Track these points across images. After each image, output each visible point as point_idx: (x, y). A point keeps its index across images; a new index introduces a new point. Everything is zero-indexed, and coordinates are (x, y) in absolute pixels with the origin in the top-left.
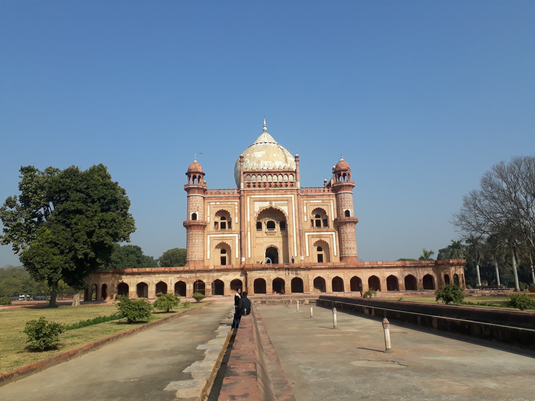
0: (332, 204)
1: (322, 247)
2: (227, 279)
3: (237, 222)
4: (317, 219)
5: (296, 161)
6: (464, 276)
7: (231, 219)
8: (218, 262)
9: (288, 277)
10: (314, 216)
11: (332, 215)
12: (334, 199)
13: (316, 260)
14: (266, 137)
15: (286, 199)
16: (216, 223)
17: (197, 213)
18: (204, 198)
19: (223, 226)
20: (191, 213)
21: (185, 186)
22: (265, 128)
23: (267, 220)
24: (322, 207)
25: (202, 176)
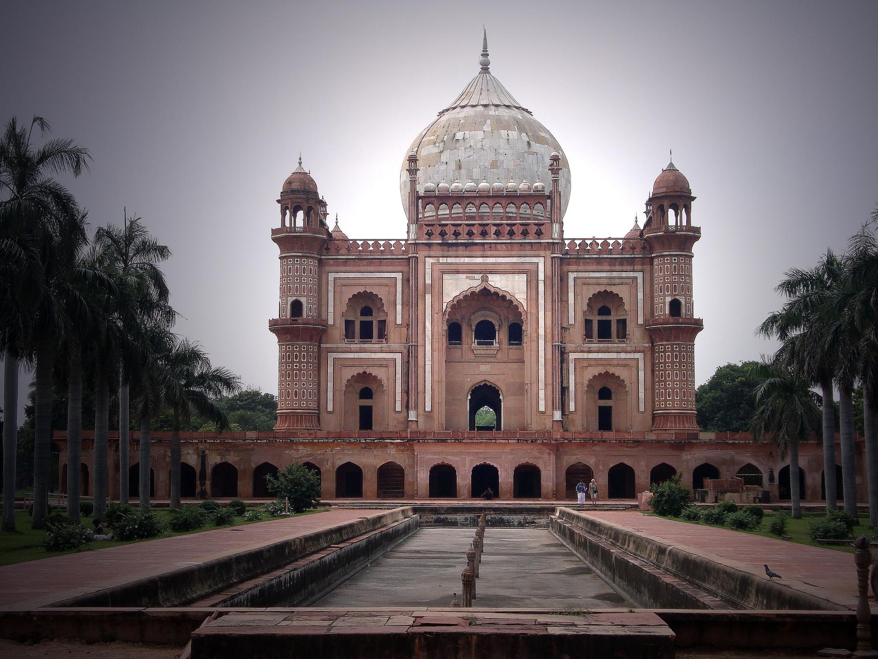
0: (640, 281)
2: (370, 461)
3: (399, 321)
4: (604, 318)
9: (506, 464)
10: (596, 312)
11: (636, 309)
17: (303, 300)
18: (320, 260)
20: (291, 300)
23: (477, 319)
24: (615, 290)
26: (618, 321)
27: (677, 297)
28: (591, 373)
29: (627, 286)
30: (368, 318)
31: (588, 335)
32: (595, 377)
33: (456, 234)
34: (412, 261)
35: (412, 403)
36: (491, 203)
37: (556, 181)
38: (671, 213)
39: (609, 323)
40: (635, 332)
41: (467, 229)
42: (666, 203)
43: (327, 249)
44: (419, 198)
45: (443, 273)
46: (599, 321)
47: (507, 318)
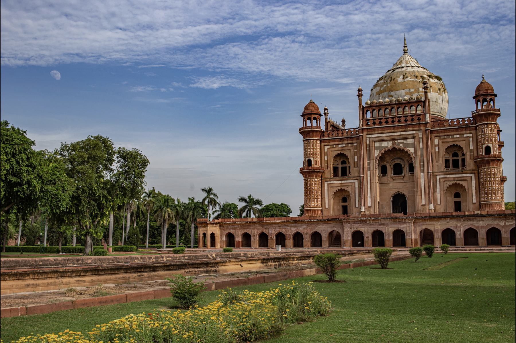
4: (455, 158)
10: (451, 156)
13: (451, 210)
15: (412, 136)
17: (312, 159)
18: (321, 141)
26: (462, 159)
29: (464, 142)
30: (344, 166)
31: (447, 166)
34: (361, 138)
37: (426, 93)
39: (458, 160)
40: (470, 164)
43: (324, 135)
44: (363, 108)
46: (453, 160)
47: (408, 161)
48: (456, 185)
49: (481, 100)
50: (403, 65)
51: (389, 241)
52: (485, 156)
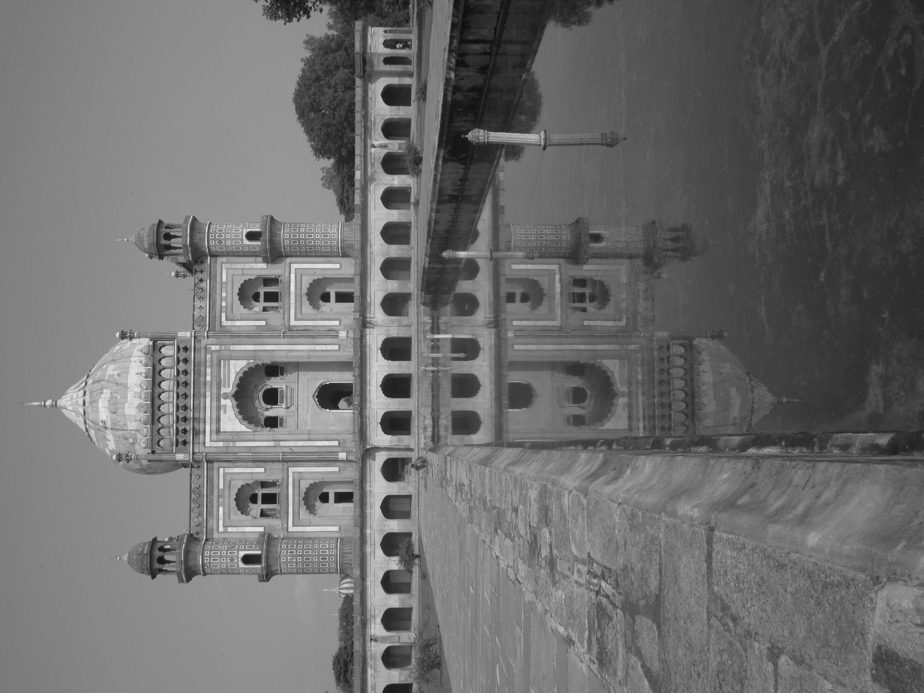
1: (319, 293)
3: (262, 470)
5: (131, 338)
6: (388, 29)
7: (256, 482)
8: (347, 507)
12: (220, 260)
14: (70, 402)
16: (263, 514)
17: (242, 554)
19: (270, 499)
20: (241, 565)
21: (181, 580)
22: (49, 403)
24: (237, 286)
25: (159, 545)
27: (244, 234)
28: (307, 308)
32: (311, 304)
33: (185, 419)
35: (331, 457)
36: (157, 391)
38: (174, 242)
39: (265, 293)
41: (181, 411)
42: (163, 242)
43: (198, 533)
44: (153, 452)
45: (218, 431)
46: (265, 301)
48: (310, 295)
49: (163, 242)
50: (81, 402)
51: (400, 366)
52: (263, 238)
